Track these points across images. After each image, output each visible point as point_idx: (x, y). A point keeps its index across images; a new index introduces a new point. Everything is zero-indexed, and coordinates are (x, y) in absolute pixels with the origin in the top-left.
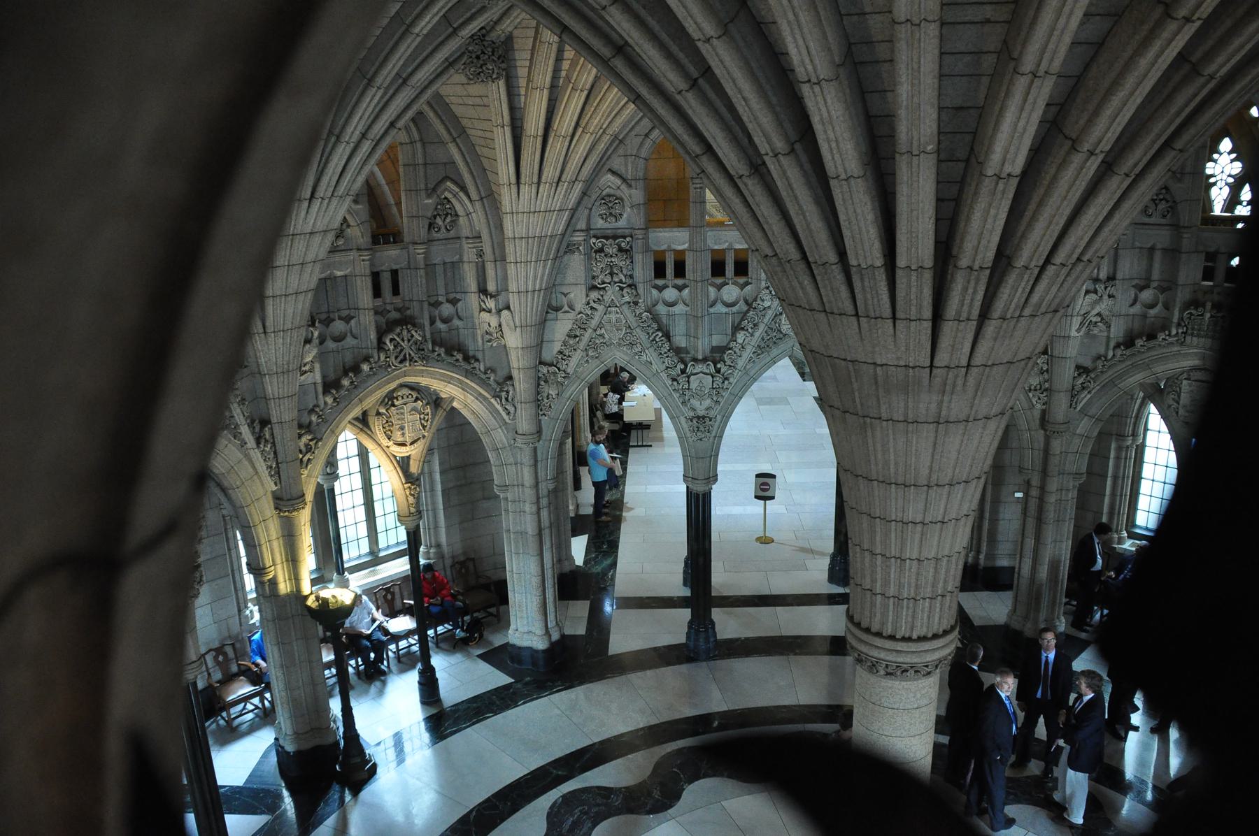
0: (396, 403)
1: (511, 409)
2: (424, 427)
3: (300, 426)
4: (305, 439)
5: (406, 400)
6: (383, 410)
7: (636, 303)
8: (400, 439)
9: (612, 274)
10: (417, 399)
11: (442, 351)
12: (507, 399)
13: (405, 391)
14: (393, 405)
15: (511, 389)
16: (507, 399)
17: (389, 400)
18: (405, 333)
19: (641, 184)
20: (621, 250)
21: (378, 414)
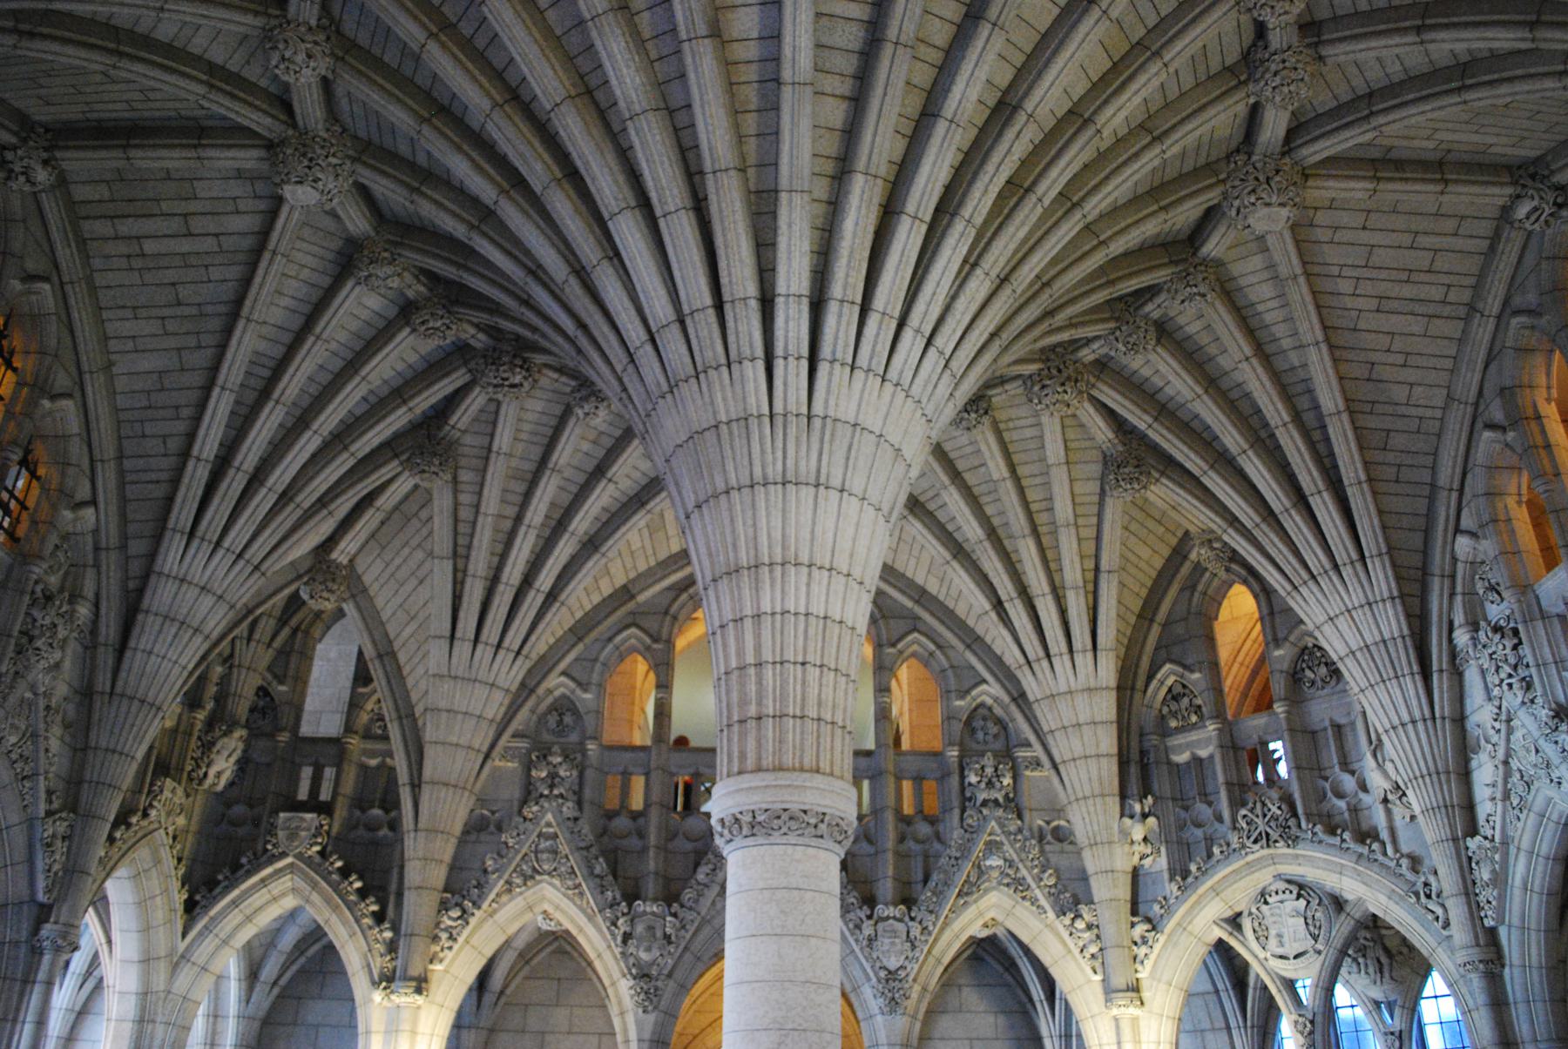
0: (1269, 900)
1: (1439, 911)
2: (1315, 938)
3: (1134, 912)
4: (1141, 929)
5: (1281, 897)
6: (1254, 910)
7: (1532, 701)
8: (1280, 951)
10: (1299, 896)
11: (1318, 828)
12: (1429, 896)
13: (1282, 886)
14: (1266, 903)
15: (1432, 879)
17: (1263, 896)
18: (1259, 805)
21: (1250, 914)
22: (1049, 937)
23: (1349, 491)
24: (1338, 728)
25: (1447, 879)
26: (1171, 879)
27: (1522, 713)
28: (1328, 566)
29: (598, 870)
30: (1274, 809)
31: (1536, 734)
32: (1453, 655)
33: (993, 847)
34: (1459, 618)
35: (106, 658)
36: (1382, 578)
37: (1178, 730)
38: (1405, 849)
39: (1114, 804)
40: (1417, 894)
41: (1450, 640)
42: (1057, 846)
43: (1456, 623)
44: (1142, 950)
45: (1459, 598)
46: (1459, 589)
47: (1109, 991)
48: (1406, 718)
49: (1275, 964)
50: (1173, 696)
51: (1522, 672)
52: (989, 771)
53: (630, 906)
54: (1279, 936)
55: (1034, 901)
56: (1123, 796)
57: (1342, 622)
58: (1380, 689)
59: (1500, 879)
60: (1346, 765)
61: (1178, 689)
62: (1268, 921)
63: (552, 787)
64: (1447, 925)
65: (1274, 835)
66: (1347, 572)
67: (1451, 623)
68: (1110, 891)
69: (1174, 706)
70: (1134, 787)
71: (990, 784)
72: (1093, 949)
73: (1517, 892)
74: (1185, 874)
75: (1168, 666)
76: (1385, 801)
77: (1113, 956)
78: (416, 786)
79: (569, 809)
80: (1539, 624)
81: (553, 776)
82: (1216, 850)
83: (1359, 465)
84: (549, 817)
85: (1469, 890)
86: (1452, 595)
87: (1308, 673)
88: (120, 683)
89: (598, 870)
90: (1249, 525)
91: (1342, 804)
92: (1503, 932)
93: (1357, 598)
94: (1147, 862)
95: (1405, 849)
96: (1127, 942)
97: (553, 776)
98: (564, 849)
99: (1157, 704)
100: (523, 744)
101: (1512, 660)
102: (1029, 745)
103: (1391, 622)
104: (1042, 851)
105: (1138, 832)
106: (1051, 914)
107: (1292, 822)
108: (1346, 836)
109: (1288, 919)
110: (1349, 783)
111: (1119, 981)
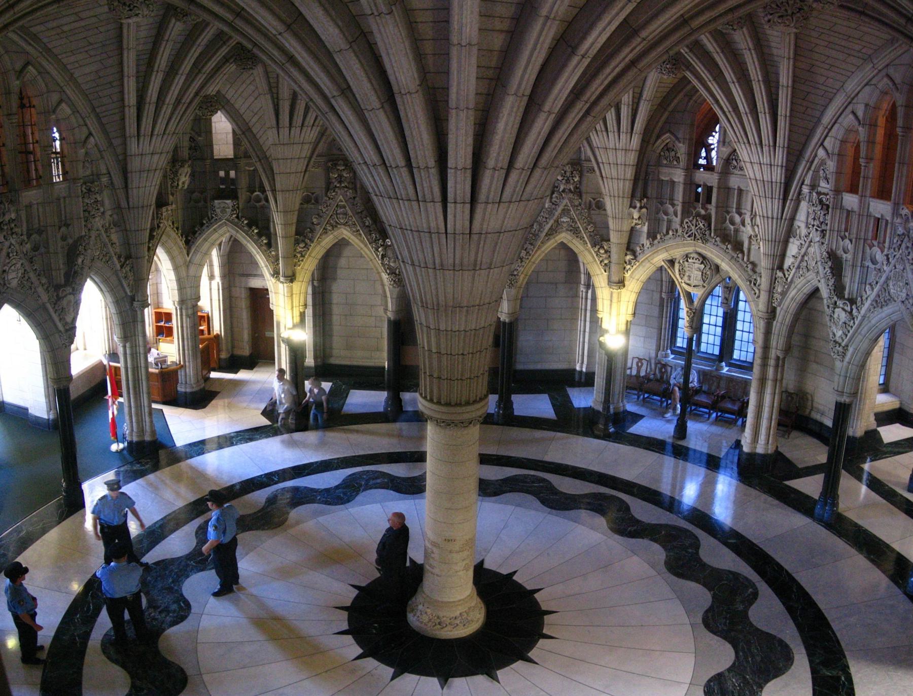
1: (757, 292)
3: (628, 249)
4: (629, 257)
7: (823, 243)
9: (814, 219)
10: (702, 263)
12: (755, 284)
13: (696, 256)
15: (758, 279)
16: (755, 284)
17: (687, 257)
19: (835, 158)
20: (821, 201)
22: (587, 253)
23: (779, 118)
24: (740, 191)
25: (764, 282)
26: (648, 238)
27: (817, 245)
28: (757, 142)
29: (367, 224)
30: (701, 225)
31: (819, 259)
32: (800, 193)
33: (565, 212)
34: (808, 181)
35: (121, 194)
36: (780, 157)
37: (666, 166)
38: (752, 259)
39: (627, 202)
40: (750, 282)
41: (801, 187)
42: (597, 211)
43: (806, 183)
44: (628, 267)
45: (811, 172)
46: (813, 168)
47: (610, 282)
48: (770, 215)
49: (683, 285)
50: (668, 148)
51: (824, 227)
52: (568, 174)
53: (384, 241)
54: (689, 277)
55: (582, 238)
56: (633, 196)
57: (756, 167)
58: (763, 200)
59: (784, 294)
60: (740, 214)
61: (670, 145)
62: (686, 269)
63: (340, 182)
64: (759, 297)
65: (698, 237)
66: (765, 149)
67: (804, 181)
68: (616, 239)
69: (667, 154)
70: (638, 194)
71: (568, 181)
72: (606, 262)
73: (789, 300)
74: (655, 238)
75: (668, 135)
76: (750, 237)
77: (614, 268)
78: (274, 191)
79: (350, 193)
80: (838, 211)
81: (340, 176)
82: (671, 233)
83: (788, 110)
84: (340, 197)
85: (771, 291)
86: (809, 169)
87: (734, 162)
88: (131, 203)
89: (367, 224)
90: (726, 109)
91: (732, 227)
92: (778, 309)
93: (766, 160)
94: (638, 227)
95: (752, 259)
96: (622, 262)
97: (340, 176)
98: (350, 213)
99: (658, 151)
100: (322, 160)
101: (821, 220)
102: (590, 161)
103: (778, 175)
104: (589, 214)
105: (636, 215)
106: (589, 245)
107: (707, 233)
108: (729, 246)
109: (695, 270)
110: (737, 219)
111: (615, 278)
